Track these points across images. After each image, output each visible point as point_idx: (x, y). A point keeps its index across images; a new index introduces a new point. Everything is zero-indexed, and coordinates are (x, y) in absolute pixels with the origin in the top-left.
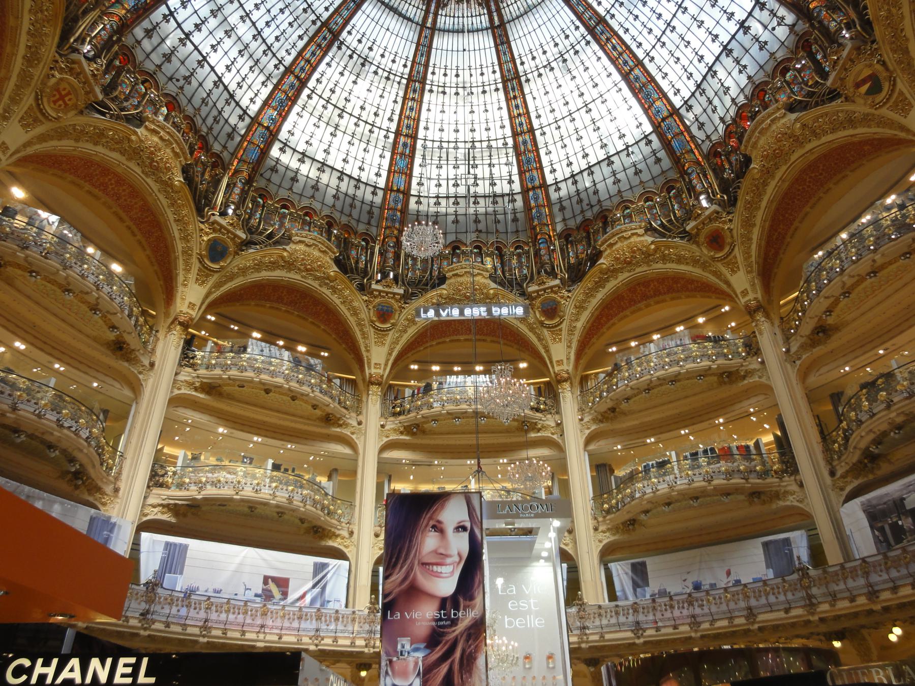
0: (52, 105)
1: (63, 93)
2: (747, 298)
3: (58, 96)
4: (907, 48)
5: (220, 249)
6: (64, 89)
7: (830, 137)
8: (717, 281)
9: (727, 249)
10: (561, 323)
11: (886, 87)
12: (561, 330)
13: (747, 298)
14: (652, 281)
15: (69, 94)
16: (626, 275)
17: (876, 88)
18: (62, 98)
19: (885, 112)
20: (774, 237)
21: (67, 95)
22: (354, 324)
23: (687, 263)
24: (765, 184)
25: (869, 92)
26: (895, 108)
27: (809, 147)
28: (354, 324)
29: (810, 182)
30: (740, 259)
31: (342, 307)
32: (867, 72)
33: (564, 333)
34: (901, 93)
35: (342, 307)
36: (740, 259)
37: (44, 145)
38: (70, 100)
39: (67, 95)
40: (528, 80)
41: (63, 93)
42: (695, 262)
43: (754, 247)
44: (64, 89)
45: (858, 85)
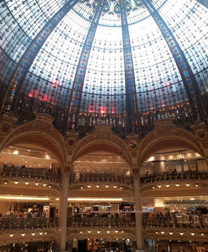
2: (69, 165)
4: (145, 147)
7: (116, 145)
8: (62, 153)
9: (72, 147)
10: (6, 136)
11: (135, 149)
12: (4, 138)
13: (69, 165)
14: (43, 138)
16: (39, 132)
17: (133, 147)
19: (130, 152)
20: (84, 152)
23: (58, 142)
24: (94, 140)
25: (131, 146)
26: (132, 154)
27: (110, 142)
29: (101, 147)
30: (73, 152)
32: (135, 143)
33: (4, 140)
34: (136, 152)
36: (73, 152)
40: (56, 31)
42: (61, 143)
43: (79, 151)
45: (131, 143)
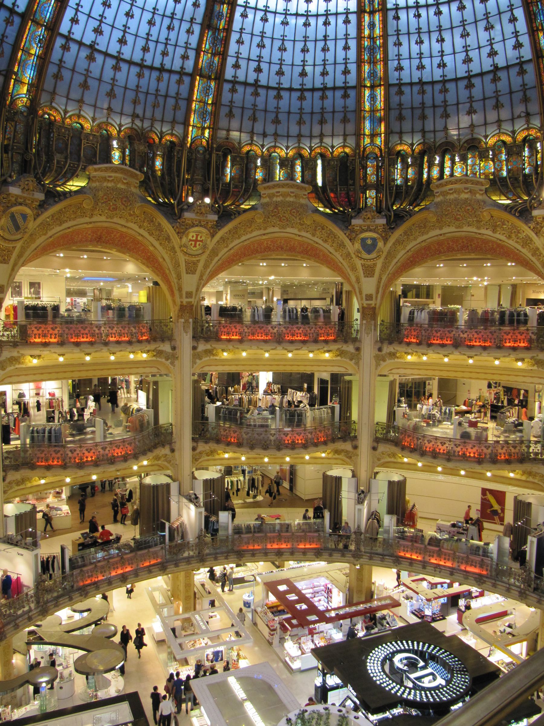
0: (195, 249)
1: (194, 238)
3: (193, 243)
5: (369, 242)
6: (193, 237)
15: (197, 236)
18: (196, 241)
21: (197, 237)
22: (529, 255)
28: (529, 255)
31: (510, 242)
35: (510, 242)
37: (211, 266)
38: (201, 237)
39: (197, 237)
41: (194, 238)
44: (193, 237)
